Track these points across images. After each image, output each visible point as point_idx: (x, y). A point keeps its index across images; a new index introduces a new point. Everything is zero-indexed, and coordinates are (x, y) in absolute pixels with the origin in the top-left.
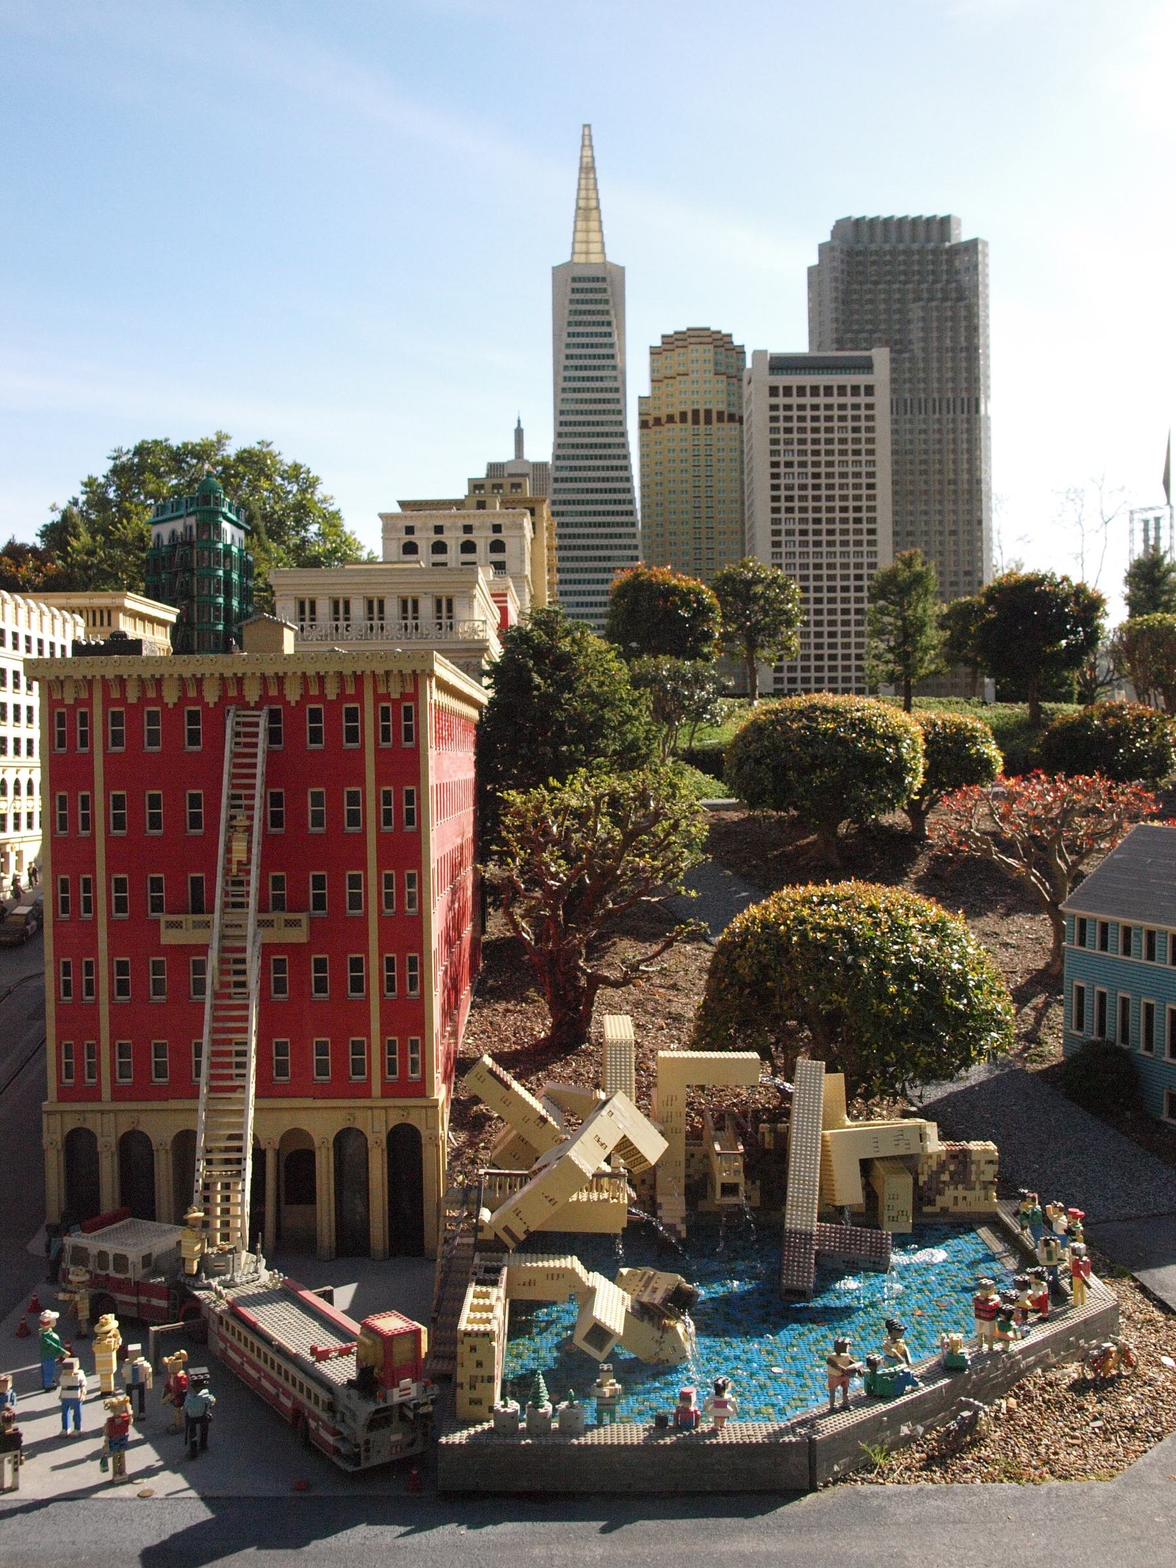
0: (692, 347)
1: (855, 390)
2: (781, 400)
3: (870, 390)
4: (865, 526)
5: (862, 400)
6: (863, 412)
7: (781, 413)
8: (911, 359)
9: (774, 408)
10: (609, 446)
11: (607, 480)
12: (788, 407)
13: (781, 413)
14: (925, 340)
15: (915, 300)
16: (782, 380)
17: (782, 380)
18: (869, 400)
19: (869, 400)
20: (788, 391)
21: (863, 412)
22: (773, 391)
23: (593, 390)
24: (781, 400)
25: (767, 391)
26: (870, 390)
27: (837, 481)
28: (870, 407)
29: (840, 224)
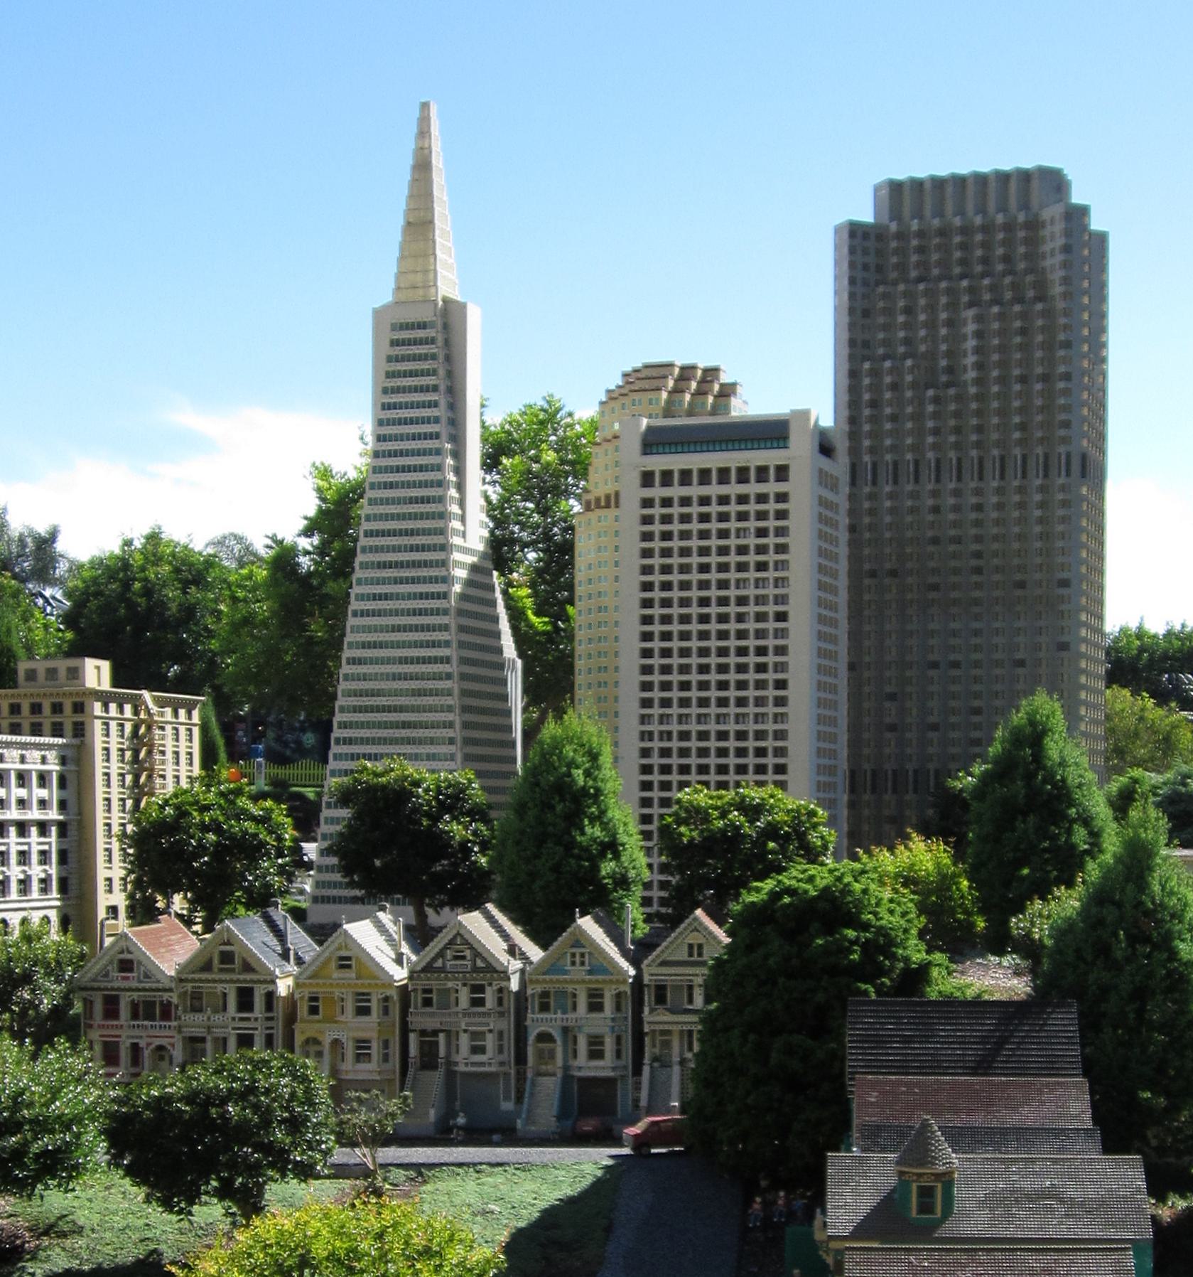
0: (636, 396)
1: (762, 473)
2: (657, 492)
3: (782, 473)
4: (770, 676)
5: (772, 487)
6: (772, 506)
7: (657, 511)
8: (959, 398)
9: (647, 503)
10: (425, 564)
11: (421, 612)
12: (667, 502)
13: (657, 511)
14: (979, 366)
15: (971, 305)
16: (658, 463)
17: (658, 463)
18: (781, 487)
19: (781, 487)
20: (667, 477)
21: (772, 506)
22: (647, 479)
23: (410, 485)
24: (657, 492)
25: (637, 480)
26: (782, 473)
27: (732, 609)
28: (782, 497)
29: (877, 189)
